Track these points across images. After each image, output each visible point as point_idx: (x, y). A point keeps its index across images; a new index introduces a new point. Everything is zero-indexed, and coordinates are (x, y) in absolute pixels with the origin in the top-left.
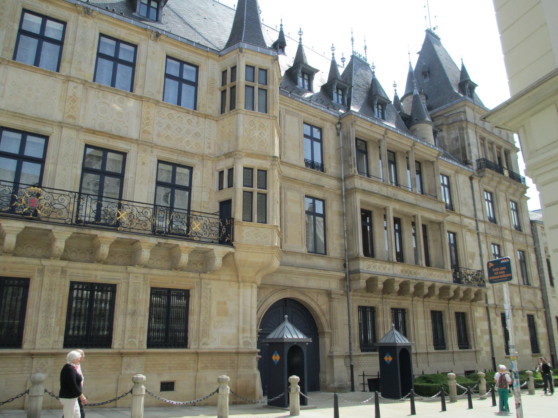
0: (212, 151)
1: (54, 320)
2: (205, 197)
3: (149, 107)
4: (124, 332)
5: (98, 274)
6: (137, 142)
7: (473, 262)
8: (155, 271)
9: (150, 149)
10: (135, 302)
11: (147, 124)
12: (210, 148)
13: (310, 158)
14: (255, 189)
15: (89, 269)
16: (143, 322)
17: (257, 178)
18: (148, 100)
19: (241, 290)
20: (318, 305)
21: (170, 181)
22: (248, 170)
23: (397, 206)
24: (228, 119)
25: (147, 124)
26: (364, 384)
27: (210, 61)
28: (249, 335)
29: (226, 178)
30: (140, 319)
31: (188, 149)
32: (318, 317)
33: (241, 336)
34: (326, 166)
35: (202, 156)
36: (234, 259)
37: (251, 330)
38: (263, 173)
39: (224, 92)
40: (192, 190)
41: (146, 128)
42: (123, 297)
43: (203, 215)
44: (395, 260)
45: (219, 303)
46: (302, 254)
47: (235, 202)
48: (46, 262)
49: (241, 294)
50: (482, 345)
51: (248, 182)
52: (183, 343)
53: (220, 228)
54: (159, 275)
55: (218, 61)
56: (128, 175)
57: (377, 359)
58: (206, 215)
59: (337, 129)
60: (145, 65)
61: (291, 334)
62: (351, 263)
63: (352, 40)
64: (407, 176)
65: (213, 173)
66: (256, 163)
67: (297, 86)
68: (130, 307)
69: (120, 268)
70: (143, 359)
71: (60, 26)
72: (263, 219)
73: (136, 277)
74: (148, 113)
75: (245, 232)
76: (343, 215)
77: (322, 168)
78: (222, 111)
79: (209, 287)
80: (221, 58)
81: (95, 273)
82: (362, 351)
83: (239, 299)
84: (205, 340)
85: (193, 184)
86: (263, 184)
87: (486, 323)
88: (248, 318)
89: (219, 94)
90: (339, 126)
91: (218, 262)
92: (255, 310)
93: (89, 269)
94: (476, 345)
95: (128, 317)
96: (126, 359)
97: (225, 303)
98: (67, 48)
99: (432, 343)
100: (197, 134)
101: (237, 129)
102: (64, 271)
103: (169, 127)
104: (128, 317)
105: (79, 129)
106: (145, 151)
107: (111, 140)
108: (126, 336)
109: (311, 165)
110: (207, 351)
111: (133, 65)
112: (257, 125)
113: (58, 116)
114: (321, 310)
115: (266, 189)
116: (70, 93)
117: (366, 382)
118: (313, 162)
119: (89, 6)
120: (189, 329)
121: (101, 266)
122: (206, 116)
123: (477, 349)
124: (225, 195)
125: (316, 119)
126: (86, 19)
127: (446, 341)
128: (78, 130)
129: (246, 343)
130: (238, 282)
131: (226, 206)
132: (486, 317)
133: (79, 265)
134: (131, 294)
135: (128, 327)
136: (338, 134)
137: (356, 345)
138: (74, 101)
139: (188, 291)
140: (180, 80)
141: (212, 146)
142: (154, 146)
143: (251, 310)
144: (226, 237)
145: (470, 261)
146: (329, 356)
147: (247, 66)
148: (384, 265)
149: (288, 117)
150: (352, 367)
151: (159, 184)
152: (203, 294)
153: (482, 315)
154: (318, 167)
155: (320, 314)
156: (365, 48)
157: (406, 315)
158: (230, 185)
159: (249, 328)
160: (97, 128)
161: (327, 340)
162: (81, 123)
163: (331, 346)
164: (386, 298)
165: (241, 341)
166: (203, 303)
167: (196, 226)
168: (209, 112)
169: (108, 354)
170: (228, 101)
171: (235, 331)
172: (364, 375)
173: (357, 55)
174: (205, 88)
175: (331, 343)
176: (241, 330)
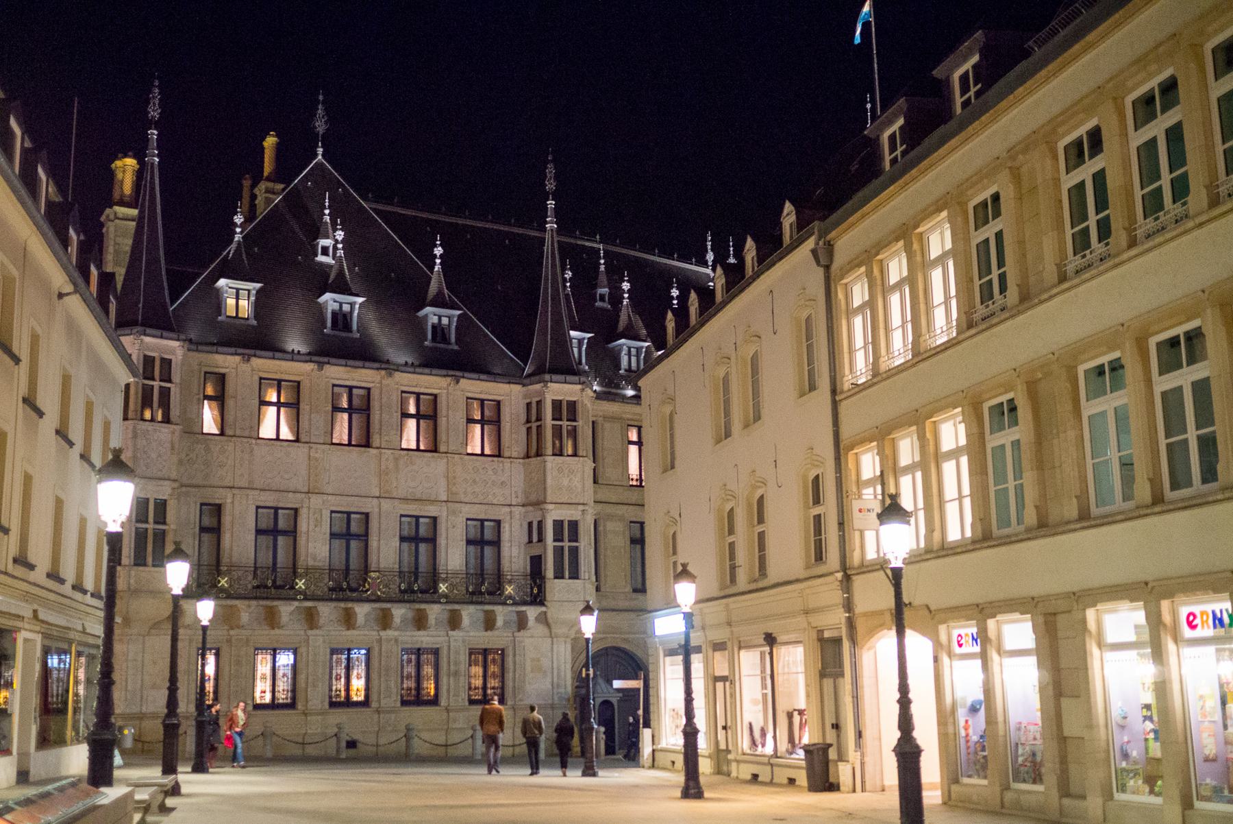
2: (515, 551)
4: (448, 691)
10: (456, 664)
22: (558, 525)
24: (534, 461)
29: (535, 532)
38: (574, 525)
39: (529, 430)
53: (532, 589)
60: (447, 416)
66: (566, 514)
68: (452, 667)
72: (575, 575)
75: (557, 588)
86: (574, 536)
89: (524, 430)
92: (569, 666)
95: (452, 679)
104: (452, 679)
124: (536, 551)
131: (536, 563)
138: (387, 474)
144: (538, 598)
149: (607, 425)
158: (540, 540)
167: (509, 590)
170: (534, 451)
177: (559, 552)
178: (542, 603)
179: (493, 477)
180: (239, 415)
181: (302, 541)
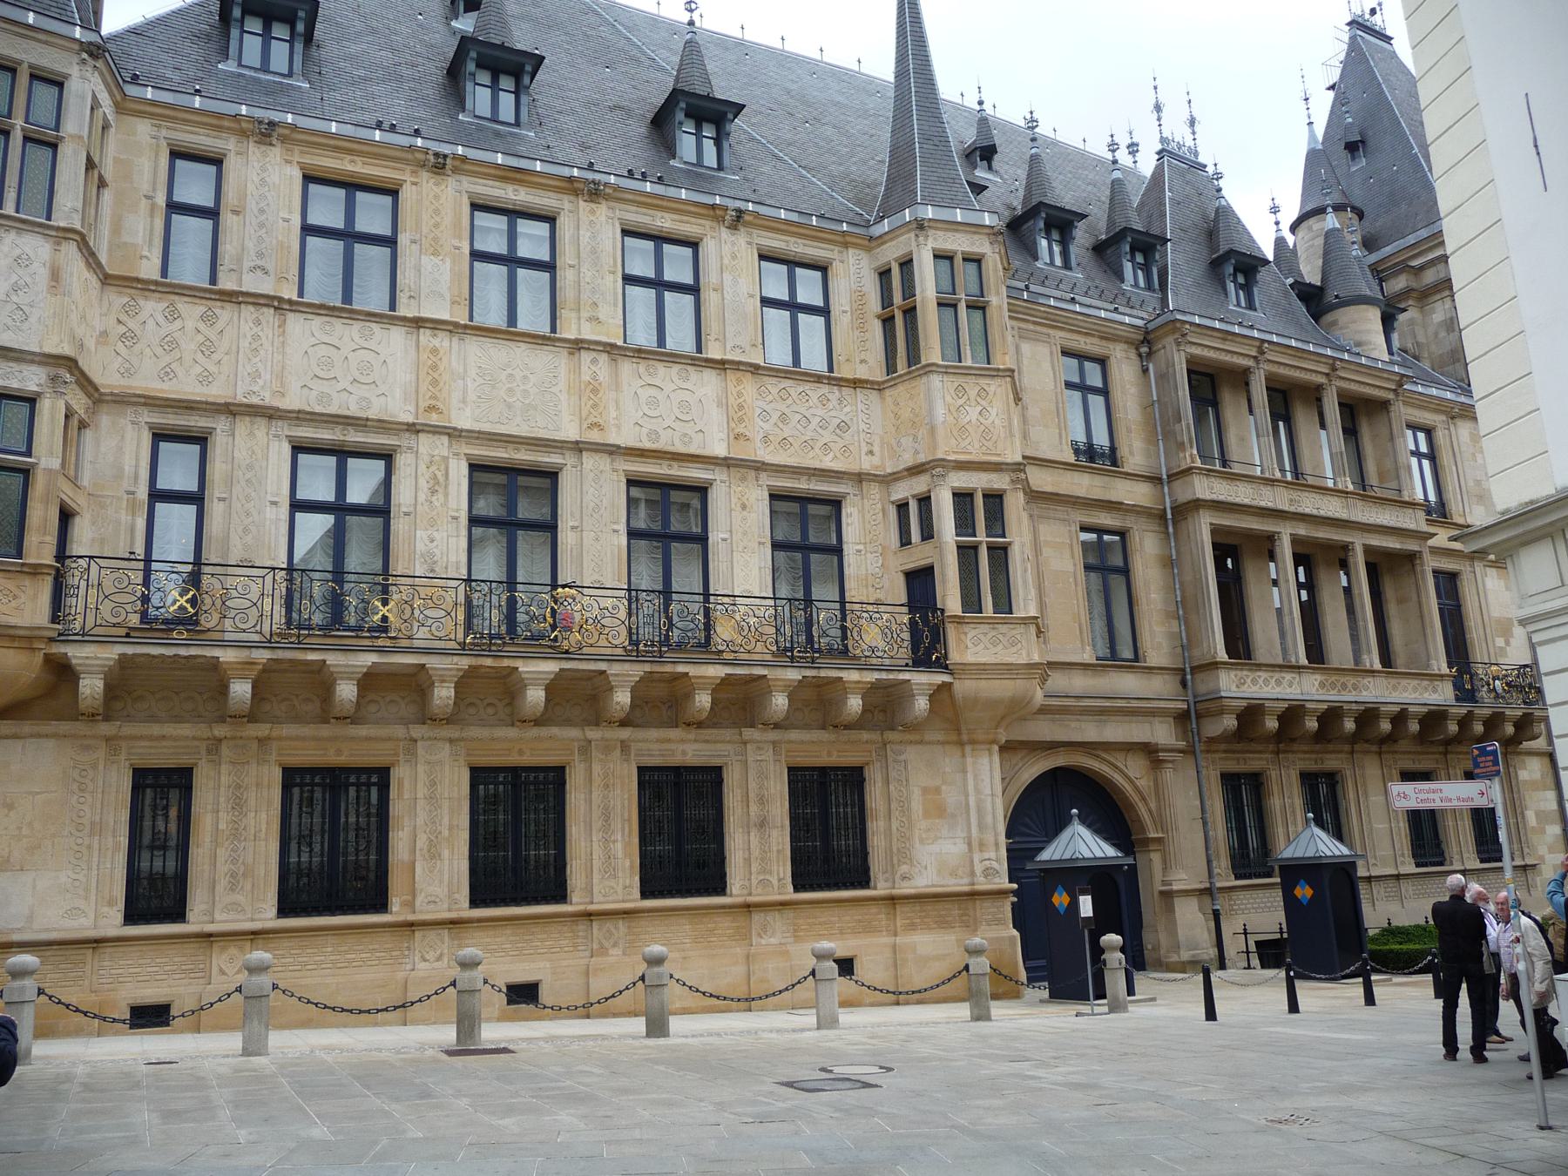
0: (876, 460)
1: (619, 845)
3: (739, 381)
4: (748, 861)
5: (683, 749)
6: (726, 463)
7: (1507, 643)
8: (794, 735)
9: (752, 473)
10: (762, 800)
11: (741, 420)
12: (871, 452)
13: (1081, 438)
14: (981, 537)
15: (669, 741)
16: (780, 839)
17: (982, 510)
18: (737, 366)
19: (969, 760)
20: (1129, 776)
21: (798, 539)
23: (1302, 530)
25: (741, 420)
26: (1248, 952)
27: (851, 251)
28: (993, 855)
29: (913, 518)
30: (775, 833)
31: (828, 463)
32: (1131, 807)
33: (977, 857)
34: (1123, 451)
35: (859, 474)
36: (952, 697)
37: (997, 844)
38: (995, 500)
39: (888, 321)
40: (845, 552)
41: (740, 430)
42: (738, 792)
43: (882, 608)
44: (1304, 661)
45: (925, 790)
46: (1085, 666)
47: (943, 574)
48: (593, 734)
49: (970, 768)
50: (1543, 850)
51: (964, 522)
52: (861, 878)
54: (802, 742)
55: (869, 250)
56: (714, 537)
57: (1277, 897)
58: (889, 609)
59: (1140, 355)
60: (719, 289)
61: (1082, 843)
62: (1199, 676)
63: (1158, 108)
64: (1323, 448)
65: (883, 510)
67: (1039, 264)
69: (728, 734)
70: (789, 914)
71: (542, 229)
72: (1004, 602)
73: (759, 748)
74: (740, 395)
76: (1170, 563)
77: (1113, 456)
78: (891, 367)
79: (902, 757)
80: (874, 244)
81: (681, 747)
82: (1237, 878)
83: (965, 780)
84: (904, 868)
85: (845, 538)
87: (1551, 795)
88: (989, 819)
89: (877, 328)
90: (1144, 350)
91: (922, 704)
93: (669, 741)
94: (1526, 850)
96: (757, 917)
97: (937, 790)
98: (566, 277)
99: (1407, 851)
100: (843, 427)
101: (931, 410)
102: (625, 746)
103: (783, 418)
105: (613, 451)
106: (743, 479)
107: (675, 464)
108: (754, 869)
109: (1088, 455)
110: (913, 891)
111: (694, 290)
112: (973, 393)
113: (570, 432)
114: (1136, 788)
115: (1004, 536)
116: (586, 377)
117: (1253, 948)
118: (1090, 445)
119: (597, 177)
120: (870, 850)
121: (692, 734)
122: (856, 384)
123: (1529, 861)
124: (918, 556)
125: (1089, 340)
126: (593, 205)
127: (1444, 846)
128: (611, 453)
129: (987, 872)
130: (961, 744)
131: (920, 581)
132: (1550, 780)
133: (653, 733)
134: (752, 785)
135: (756, 853)
136: (1145, 371)
137: (1223, 864)
138: (595, 391)
139: (861, 769)
140: (793, 307)
141: (876, 449)
142: (759, 467)
143: (993, 803)
145: (1500, 642)
146: (1162, 893)
147: (935, 256)
148: (1277, 675)
150: (1216, 915)
151: (776, 546)
152: (893, 774)
153: (1537, 776)
154: (1103, 455)
155: (1135, 798)
156: (1192, 122)
157: (1339, 787)
158: (928, 534)
159: (992, 840)
160: (648, 445)
161: (1156, 858)
162: (613, 438)
163: (1165, 869)
164: (1285, 752)
165: (978, 869)
166: (894, 794)
168: (862, 373)
169: (723, 907)
171: (965, 847)
172: (1245, 933)
173: (1173, 147)
174: (846, 319)
175: (1164, 861)
176: (975, 844)
177: (967, 553)
178: (942, 665)
179: (820, 412)
180: (250, 244)
181: (399, 526)
